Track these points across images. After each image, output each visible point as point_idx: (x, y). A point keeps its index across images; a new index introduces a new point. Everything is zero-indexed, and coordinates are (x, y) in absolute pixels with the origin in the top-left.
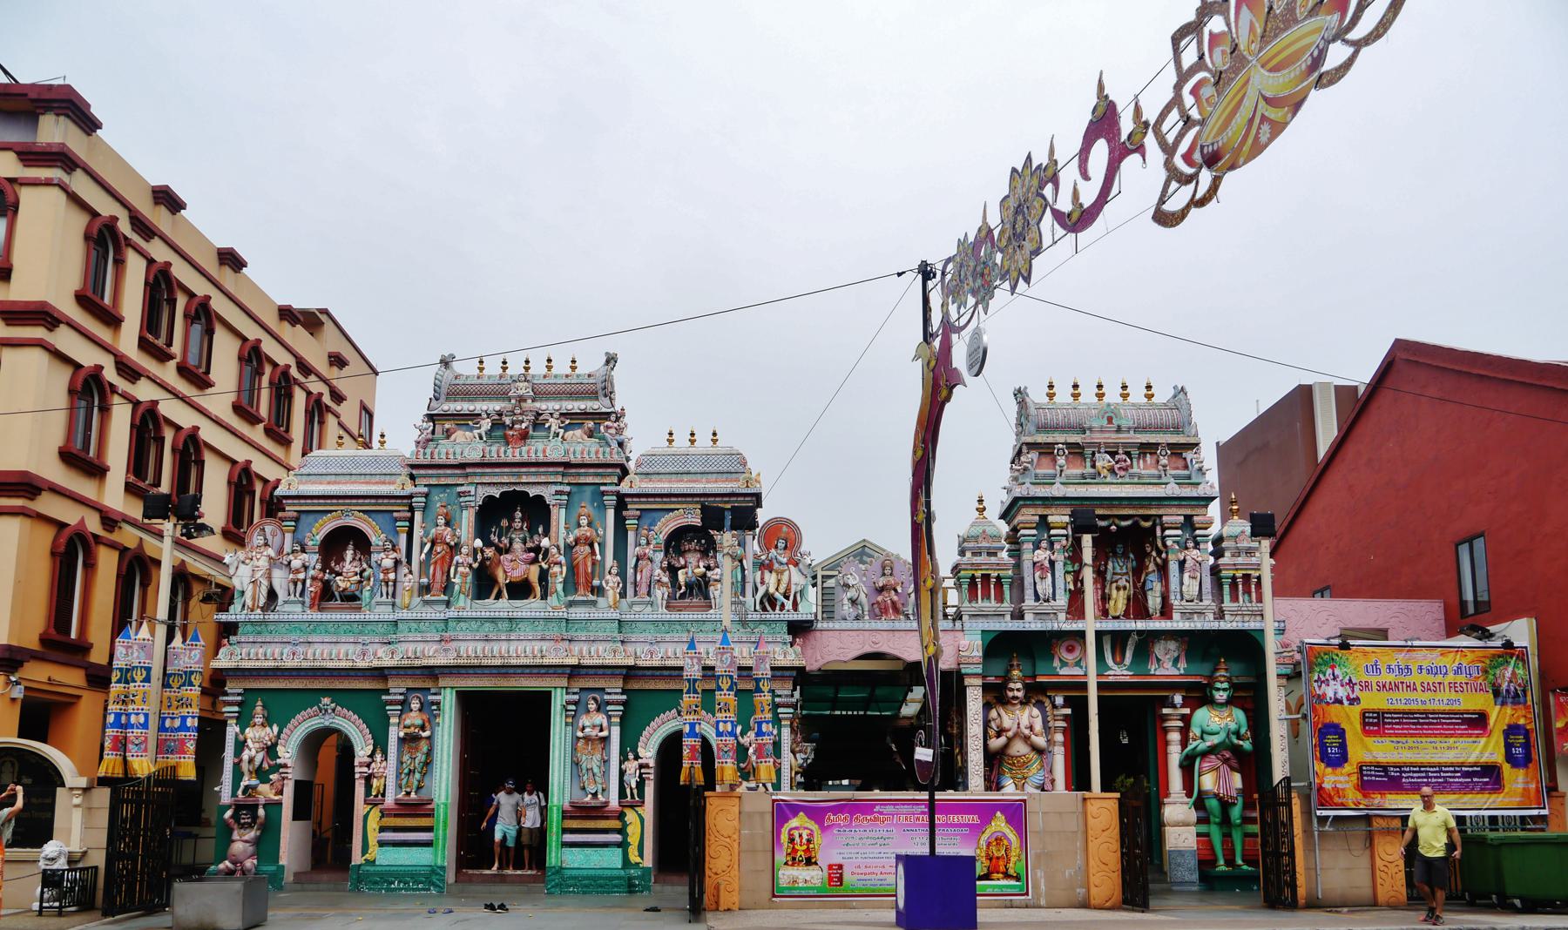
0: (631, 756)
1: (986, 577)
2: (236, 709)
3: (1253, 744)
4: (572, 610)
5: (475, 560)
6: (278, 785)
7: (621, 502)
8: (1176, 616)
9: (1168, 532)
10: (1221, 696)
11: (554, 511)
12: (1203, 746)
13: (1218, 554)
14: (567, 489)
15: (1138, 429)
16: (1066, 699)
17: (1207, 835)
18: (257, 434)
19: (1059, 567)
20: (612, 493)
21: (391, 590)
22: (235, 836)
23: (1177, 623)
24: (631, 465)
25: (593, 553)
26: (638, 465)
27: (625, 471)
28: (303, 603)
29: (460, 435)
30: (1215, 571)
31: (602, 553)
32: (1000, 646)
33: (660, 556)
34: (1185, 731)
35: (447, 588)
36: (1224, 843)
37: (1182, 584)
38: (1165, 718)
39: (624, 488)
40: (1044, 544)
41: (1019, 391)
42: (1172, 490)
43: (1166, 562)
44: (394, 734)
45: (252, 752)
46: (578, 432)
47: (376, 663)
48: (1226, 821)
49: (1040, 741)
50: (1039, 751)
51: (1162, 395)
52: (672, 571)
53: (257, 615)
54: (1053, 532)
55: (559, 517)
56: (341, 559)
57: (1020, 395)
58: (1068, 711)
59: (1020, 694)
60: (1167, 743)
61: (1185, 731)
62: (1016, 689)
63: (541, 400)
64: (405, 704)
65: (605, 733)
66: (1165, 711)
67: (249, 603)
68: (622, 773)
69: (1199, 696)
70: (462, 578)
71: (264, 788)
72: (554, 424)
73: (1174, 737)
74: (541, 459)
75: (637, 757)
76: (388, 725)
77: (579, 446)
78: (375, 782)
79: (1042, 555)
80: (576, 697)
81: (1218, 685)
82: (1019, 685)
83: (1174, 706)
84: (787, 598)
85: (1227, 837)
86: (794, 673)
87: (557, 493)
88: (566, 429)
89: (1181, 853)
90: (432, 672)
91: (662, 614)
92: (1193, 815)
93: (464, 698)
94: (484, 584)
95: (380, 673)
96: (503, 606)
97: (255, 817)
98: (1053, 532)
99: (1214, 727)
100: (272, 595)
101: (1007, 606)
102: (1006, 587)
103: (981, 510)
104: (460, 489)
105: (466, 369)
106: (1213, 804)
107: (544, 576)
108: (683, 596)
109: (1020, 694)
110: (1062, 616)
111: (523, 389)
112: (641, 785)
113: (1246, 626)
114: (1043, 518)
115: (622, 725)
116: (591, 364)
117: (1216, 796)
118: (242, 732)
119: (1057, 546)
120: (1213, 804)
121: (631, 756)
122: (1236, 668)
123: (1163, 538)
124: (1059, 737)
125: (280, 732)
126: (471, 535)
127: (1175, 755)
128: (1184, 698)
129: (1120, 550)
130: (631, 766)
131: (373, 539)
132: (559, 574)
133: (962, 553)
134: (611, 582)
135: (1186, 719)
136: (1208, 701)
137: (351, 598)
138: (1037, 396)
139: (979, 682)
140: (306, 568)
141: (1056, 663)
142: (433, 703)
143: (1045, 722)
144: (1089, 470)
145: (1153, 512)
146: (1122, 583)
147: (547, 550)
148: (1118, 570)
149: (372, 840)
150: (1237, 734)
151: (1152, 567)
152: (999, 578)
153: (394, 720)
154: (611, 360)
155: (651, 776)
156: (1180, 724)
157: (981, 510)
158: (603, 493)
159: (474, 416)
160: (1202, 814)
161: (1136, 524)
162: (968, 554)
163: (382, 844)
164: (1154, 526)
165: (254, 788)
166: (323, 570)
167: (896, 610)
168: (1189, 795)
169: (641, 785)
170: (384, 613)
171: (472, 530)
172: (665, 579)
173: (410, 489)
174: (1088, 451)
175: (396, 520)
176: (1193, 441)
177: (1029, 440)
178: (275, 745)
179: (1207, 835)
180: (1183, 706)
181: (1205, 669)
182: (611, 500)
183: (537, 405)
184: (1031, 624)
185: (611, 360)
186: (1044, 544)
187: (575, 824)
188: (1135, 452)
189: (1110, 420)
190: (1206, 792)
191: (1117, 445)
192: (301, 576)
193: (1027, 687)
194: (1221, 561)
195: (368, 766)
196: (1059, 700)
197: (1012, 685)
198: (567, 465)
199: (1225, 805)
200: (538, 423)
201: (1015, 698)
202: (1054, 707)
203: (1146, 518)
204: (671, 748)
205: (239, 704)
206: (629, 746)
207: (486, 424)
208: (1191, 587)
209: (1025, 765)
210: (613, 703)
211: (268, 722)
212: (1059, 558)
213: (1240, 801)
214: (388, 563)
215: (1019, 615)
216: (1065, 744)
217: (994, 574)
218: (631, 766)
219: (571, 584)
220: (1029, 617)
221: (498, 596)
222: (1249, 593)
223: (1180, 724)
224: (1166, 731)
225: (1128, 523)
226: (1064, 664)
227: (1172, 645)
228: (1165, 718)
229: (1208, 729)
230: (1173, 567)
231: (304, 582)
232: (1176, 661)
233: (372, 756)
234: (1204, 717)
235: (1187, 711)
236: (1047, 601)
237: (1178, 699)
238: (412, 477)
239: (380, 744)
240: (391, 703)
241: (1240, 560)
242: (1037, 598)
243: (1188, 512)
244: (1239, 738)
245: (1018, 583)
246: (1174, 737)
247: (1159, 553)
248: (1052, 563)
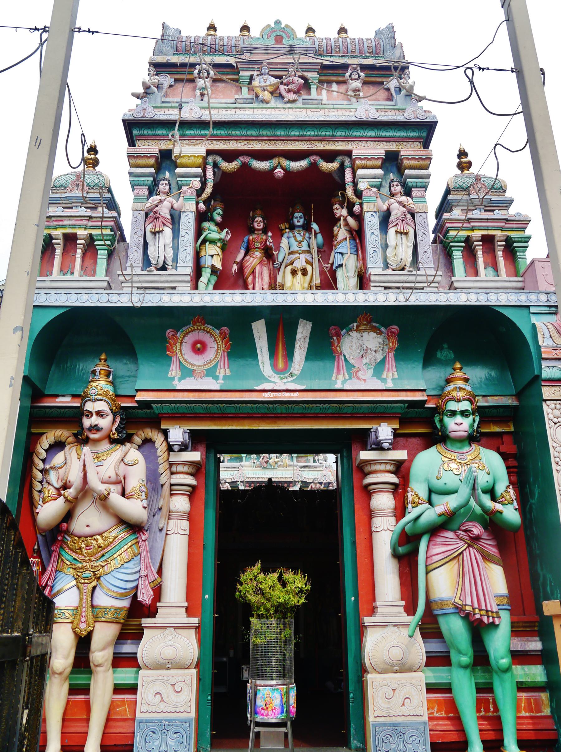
12: (430, 515)
16: (193, 434)
17: (447, 689)
23: (375, 297)
34: (400, 490)
36: (480, 704)
37: (385, 246)
42: (367, 109)
43: (359, 218)
48: (481, 659)
49: (135, 509)
50: (135, 528)
58: (196, 456)
59: (105, 423)
60: (370, 514)
61: (400, 490)
66: (365, 455)
69: (422, 424)
73: (383, 501)
81: (452, 406)
83: (379, 447)
85: (484, 689)
89: (397, 730)
92: (419, 649)
99: (449, 480)
106: (455, 628)
113: (493, 299)
114: (166, 155)
117: (459, 610)
120: (455, 628)
122: (478, 374)
124: (181, 503)
127: (385, 533)
128: (396, 434)
129: (299, 219)
135: (401, 469)
136: (437, 437)
141: (174, 371)
143: (152, 477)
146: (300, 263)
148: (295, 248)
150: (491, 492)
156: (394, 479)
160: (435, 646)
164: (342, 168)
168: (411, 609)
174: (245, 75)
179: (447, 689)
180: (394, 446)
186: (163, 187)
188: (313, 76)
189: (279, 40)
190: (442, 603)
199: (478, 630)
201: (95, 428)
203: (329, 156)
208: (400, 249)
209: (101, 552)
213: (505, 621)
216: (190, 517)
222: (495, 267)
223: (394, 479)
224: (368, 492)
225: (303, 164)
226: (187, 372)
227: (372, 340)
229: (439, 484)
230: (372, 223)
232: (380, 366)
234: (430, 464)
235: (401, 455)
236: (164, 268)
237: (385, 431)
241: (476, 214)
242: (147, 261)
243: (393, 147)
244: (494, 498)
246: (383, 501)
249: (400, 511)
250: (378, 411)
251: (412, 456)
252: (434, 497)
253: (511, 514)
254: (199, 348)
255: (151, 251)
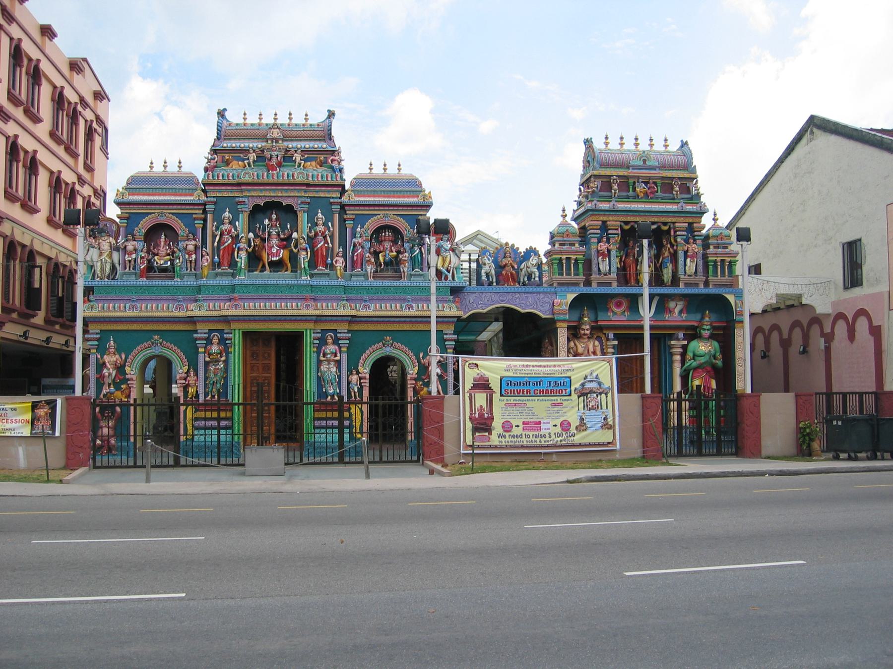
0: (354, 372)
1: (568, 259)
2: (96, 343)
3: (723, 362)
4: (314, 279)
5: (249, 246)
6: (127, 391)
7: (343, 207)
8: (682, 285)
9: (678, 233)
10: (706, 333)
11: (300, 215)
12: (695, 364)
13: (706, 246)
14: (308, 200)
15: (663, 167)
16: (615, 335)
18: (60, 150)
19: (613, 253)
20: (337, 203)
21: (193, 265)
22: (103, 424)
23: (682, 289)
24: (347, 187)
25: (326, 242)
26: (352, 185)
27: (343, 191)
28: (135, 274)
29: (235, 164)
30: (705, 257)
31: (332, 243)
32: (579, 303)
33: (367, 245)
35: (233, 264)
37: (685, 265)
38: (671, 347)
39: (345, 200)
40: (604, 239)
41: (587, 140)
43: (676, 252)
44: (202, 359)
45: (109, 372)
46: (314, 163)
47: (189, 314)
51: (674, 147)
52: (376, 254)
53: (106, 282)
54: (610, 232)
55: (303, 218)
56: (157, 245)
57: (588, 143)
58: (616, 342)
59: (588, 332)
60: (672, 362)
62: (586, 329)
63: (287, 141)
64: (209, 341)
65: (338, 358)
66: (673, 342)
67: (98, 272)
68: (349, 383)
69: (693, 334)
70: (242, 259)
71: (118, 394)
72: (297, 157)
73: (678, 358)
74: (291, 181)
75: (358, 373)
76: (198, 353)
77: (314, 172)
78: (190, 390)
79: (603, 247)
80: (320, 335)
81: (705, 327)
82: (588, 327)
83: (678, 339)
84: (449, 272)
86: (456, 319)
87: (302, 203)
88: (306, 160)
90: (226, 320)
91: (371, 282)
93: (246, 335)
94: (254, 260)
95: (192, 320)
96: (268, 277)
97: (114, 412)
98: (610, 232)
100: (113, 268)
101: (582, 277)
102: (581, 266)
103: (564, 216)
104: (237, 200)
105: (234, 117)
107: (294, 258)
108: (382, 270)
109: (588, 332)
110: (615, 284)
111: (276, 133)
112: (361, 390)
115: (348, 352)
116: (318, 118)
118: (102, 357)
119: (612, 241)
121: (354, 372)
122: (714, 317)
123: (675, 236)
125: (126, 358)
126: (246, 230)
130: (354, 378)
131: (180, 232)
132: (304, 258)
133: (552, 243)
134: (339, 263)
135: (685, 348)
137: (164, 270)
138: (598, 145)
139: (565, 325)
140: (135, 250)
142: (227, 339)
143: (602, 349)
144: (631, 192)
145: (669, 220)
147: (296, 240)
149: (189, 427)
150: (715, 357)
151: (667, 254)
152: (576, 260)
153: (201, 350)
154: (331, 114)
155: (366, 384)
157: (564, 216)
158: (331, 204)
159: (246, 151)
161: (659, 227)
162: (557, 245)
163: (195, 428)
165: (112, 393)
166: (148, 252)
167: (514, 280)
169: (361, 390)
170: (190, 281)
171: (246, 227)
172: (373, 260)
173: (203, 198)
175: (195, 219)
176: (693, 176)
177: (596, 173)
178: (124, 365)
181: (698, 317)
182: (336, 208)
183: (286, 144)
184: (594, 289)
185: (331, 114)
187: (323, 415)
189: (644, 161)
191: (650, 178)
192: (134, 256)
193: (593, 328)
194: (708, 251)
195: (185, 379)
196: (611, 336)
197: (584, 327)
198: (308, 185)
200: (287, 158)
201: (585, 334)
202: (608, 339)
203: (665, 224)
204: (381, 366)
205: (97, 340)
206: (353, 367)
207: (252, 156)
208: (691, 266)
210: (343, 339)
211: (118, 351)
212: (614, 249)
214: (191, 248)
215: (588, 283)
217: (574, 257)
218: (354, 378)
219: (313, 264)
220: (594, 285)
221: (263, 269)
224: (672, 355)
228: (671, 347)
230: (681, 255)
231: (135, 260)
233: (188, 372)
235: (685, 342)
237: (681, 335)
238: (204, 191)
239: (193, 364)
240: (200, 339)
245: (588, 263)
247: (672, 246)
248: (609, 251)
249: (683, 362)
250: (679, 328)
251: (688, 343)
252: (696, 358)
253: (719, 363)
254: (618, 305)
255: (601, 267)
